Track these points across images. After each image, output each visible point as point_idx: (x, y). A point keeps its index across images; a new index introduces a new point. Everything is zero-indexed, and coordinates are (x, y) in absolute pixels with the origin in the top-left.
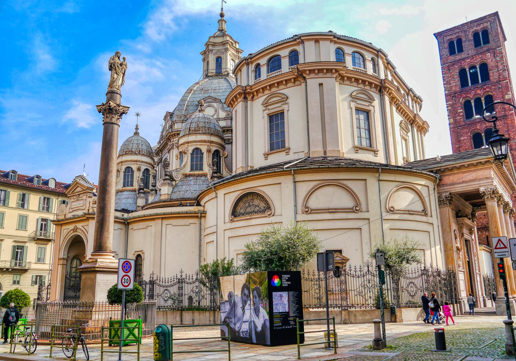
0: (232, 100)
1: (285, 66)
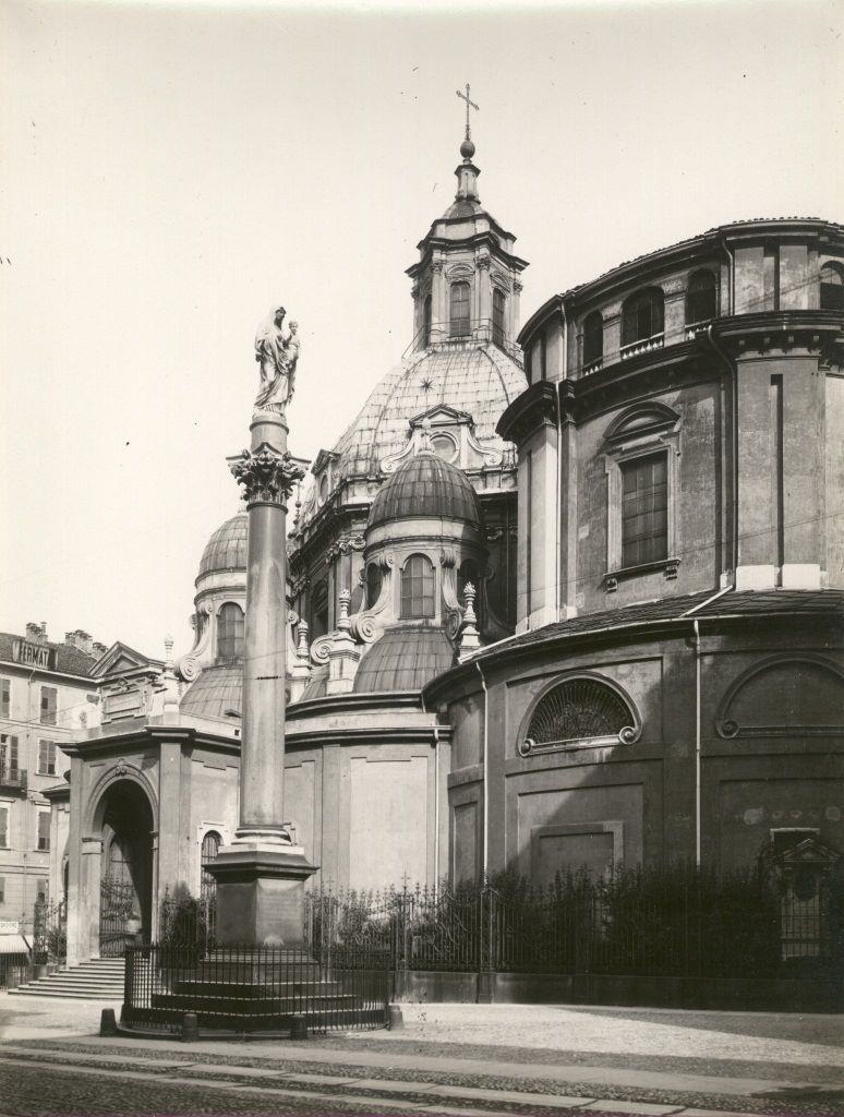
1: (675, 328)
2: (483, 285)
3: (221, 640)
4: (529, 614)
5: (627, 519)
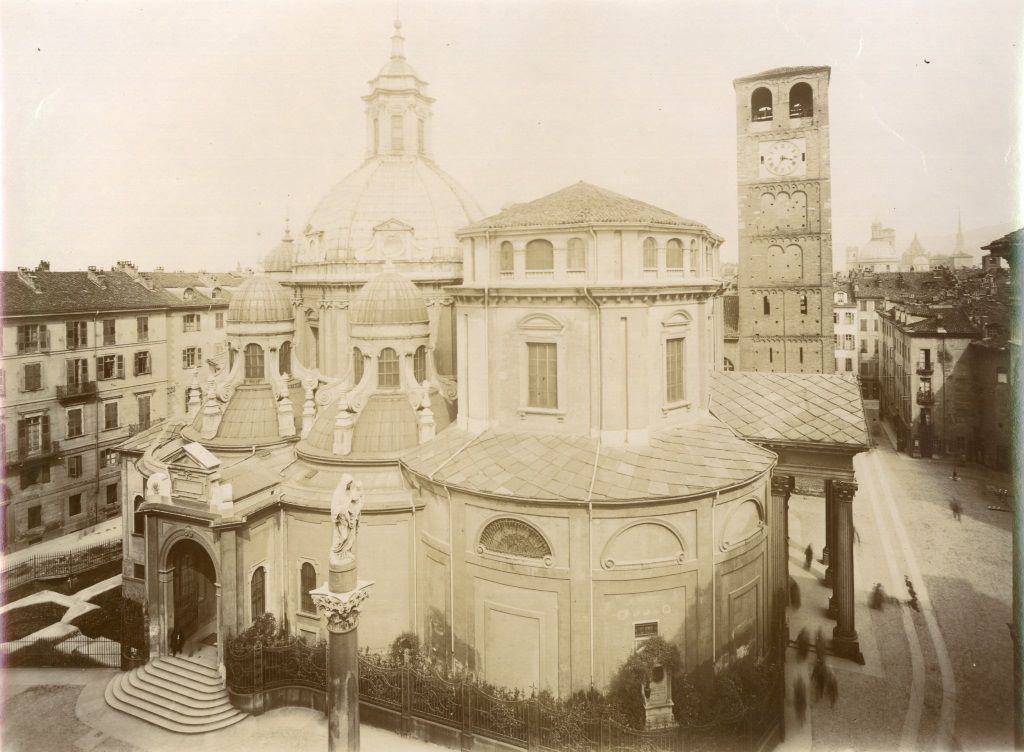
2: (410, 120)
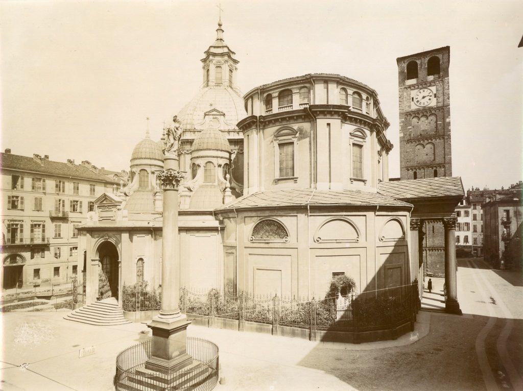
0: (245, 125)
2: (226, 68)
3: (140, 181)
4: (248, 187)
5: (281, 163)
